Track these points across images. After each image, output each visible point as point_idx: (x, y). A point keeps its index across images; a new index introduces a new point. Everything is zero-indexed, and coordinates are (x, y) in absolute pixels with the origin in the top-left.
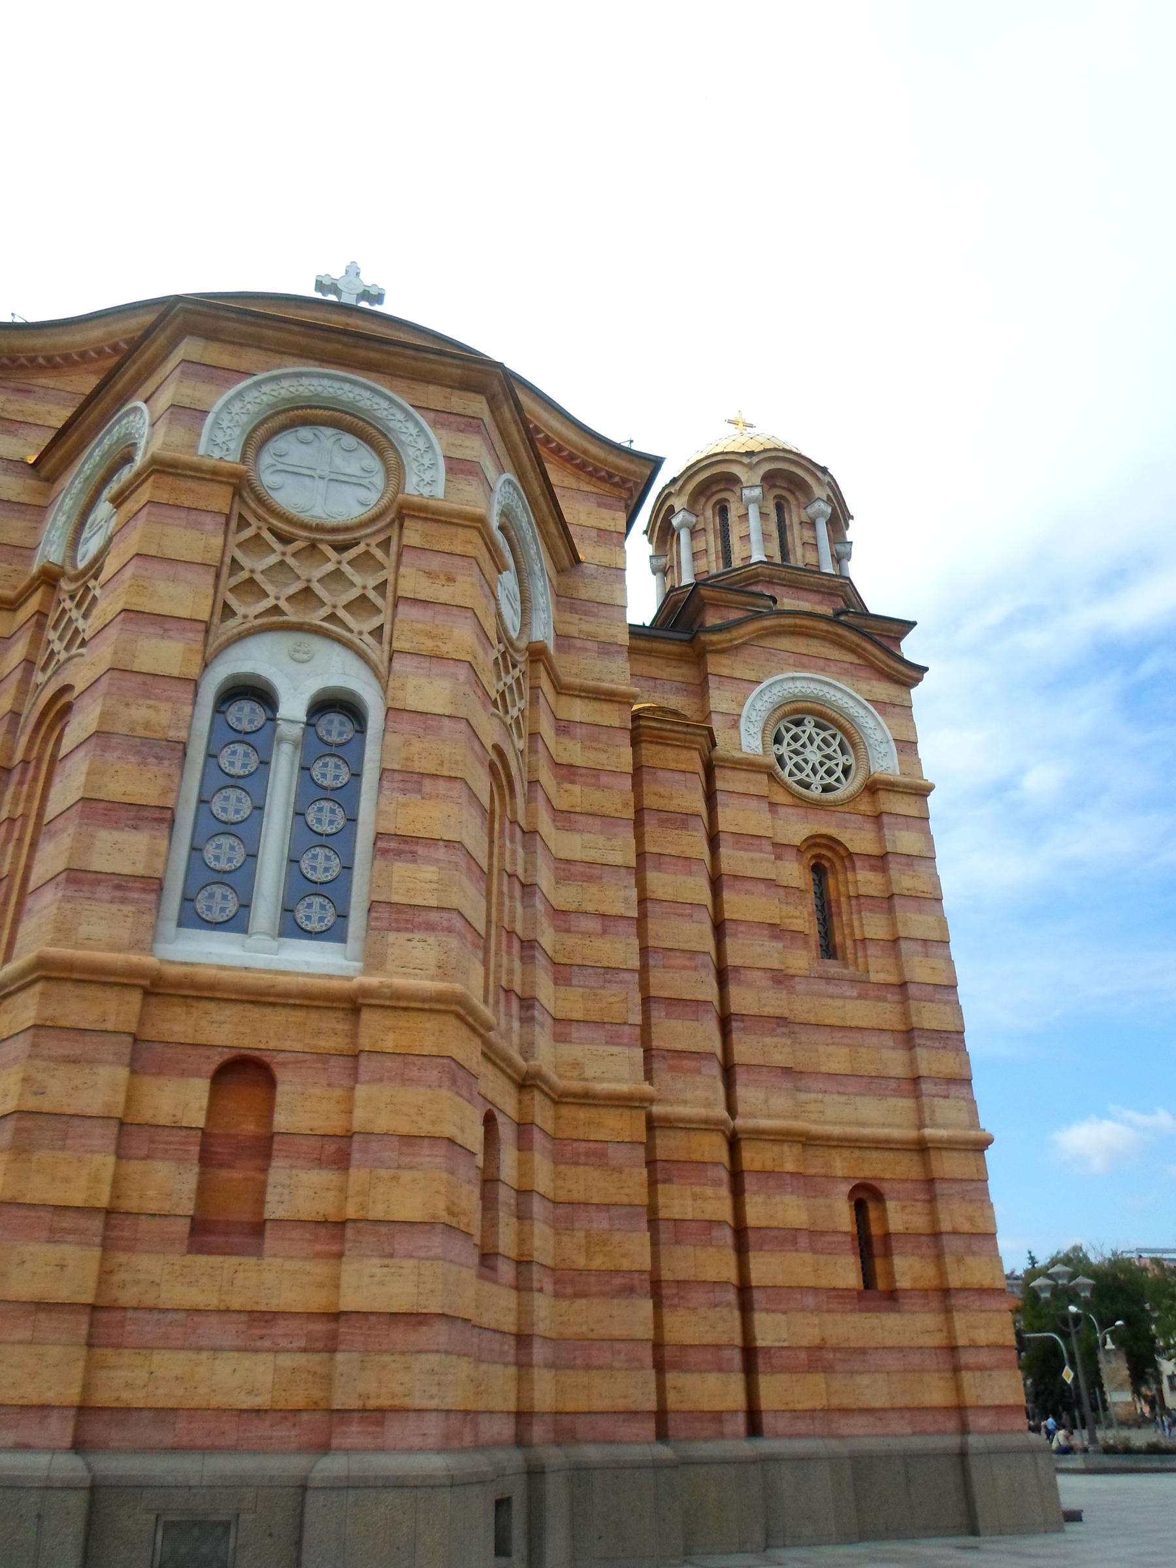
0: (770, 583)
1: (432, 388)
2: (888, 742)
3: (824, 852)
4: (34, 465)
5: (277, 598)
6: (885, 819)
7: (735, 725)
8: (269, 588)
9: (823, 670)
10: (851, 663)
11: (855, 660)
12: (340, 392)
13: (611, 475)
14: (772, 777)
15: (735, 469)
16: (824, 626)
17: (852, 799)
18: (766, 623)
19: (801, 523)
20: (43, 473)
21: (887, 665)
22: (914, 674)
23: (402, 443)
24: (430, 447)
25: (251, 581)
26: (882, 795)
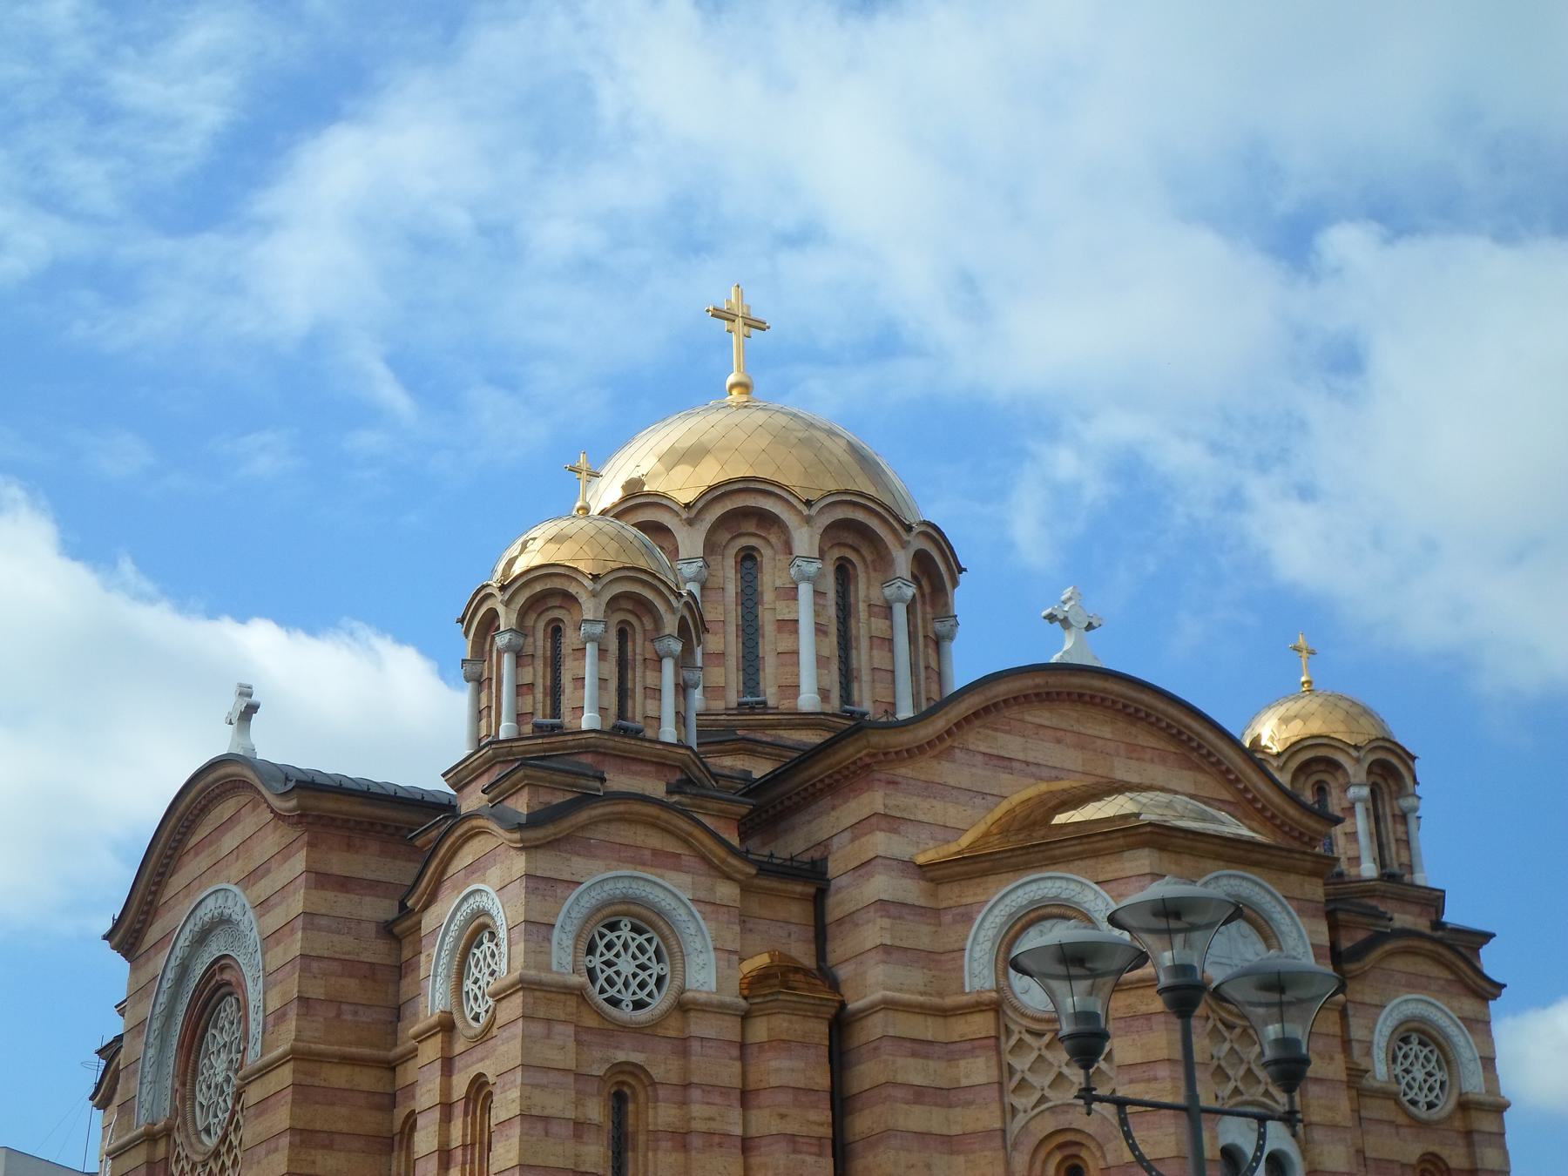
0: (1383, 896)
1: (1292, 877)
2: (1475, 1060)
3: (1428, 1166)
4: (920, 866)
5: (1236, 1081)
6: (1476, 1137)
7: (1368, 1053)
8: (1230, 1072)
9: (1425, 988)
10: (1447, 980)
11: (1450, 977)
12: (1241, 889)
13: (1301, 834)
14: (1398, 1103)
15: (1340, 757)
16: (1428, 946)
17: (1450, 1117)
18: (1388, 947)
19: (1394, 816)
20: (930, 875)
21: (1475, 983)
22: (1494, 991)
23: (1282, 933)
24: (1301, 936)
25: (1219, 1066)
26: (1473, 1113)
